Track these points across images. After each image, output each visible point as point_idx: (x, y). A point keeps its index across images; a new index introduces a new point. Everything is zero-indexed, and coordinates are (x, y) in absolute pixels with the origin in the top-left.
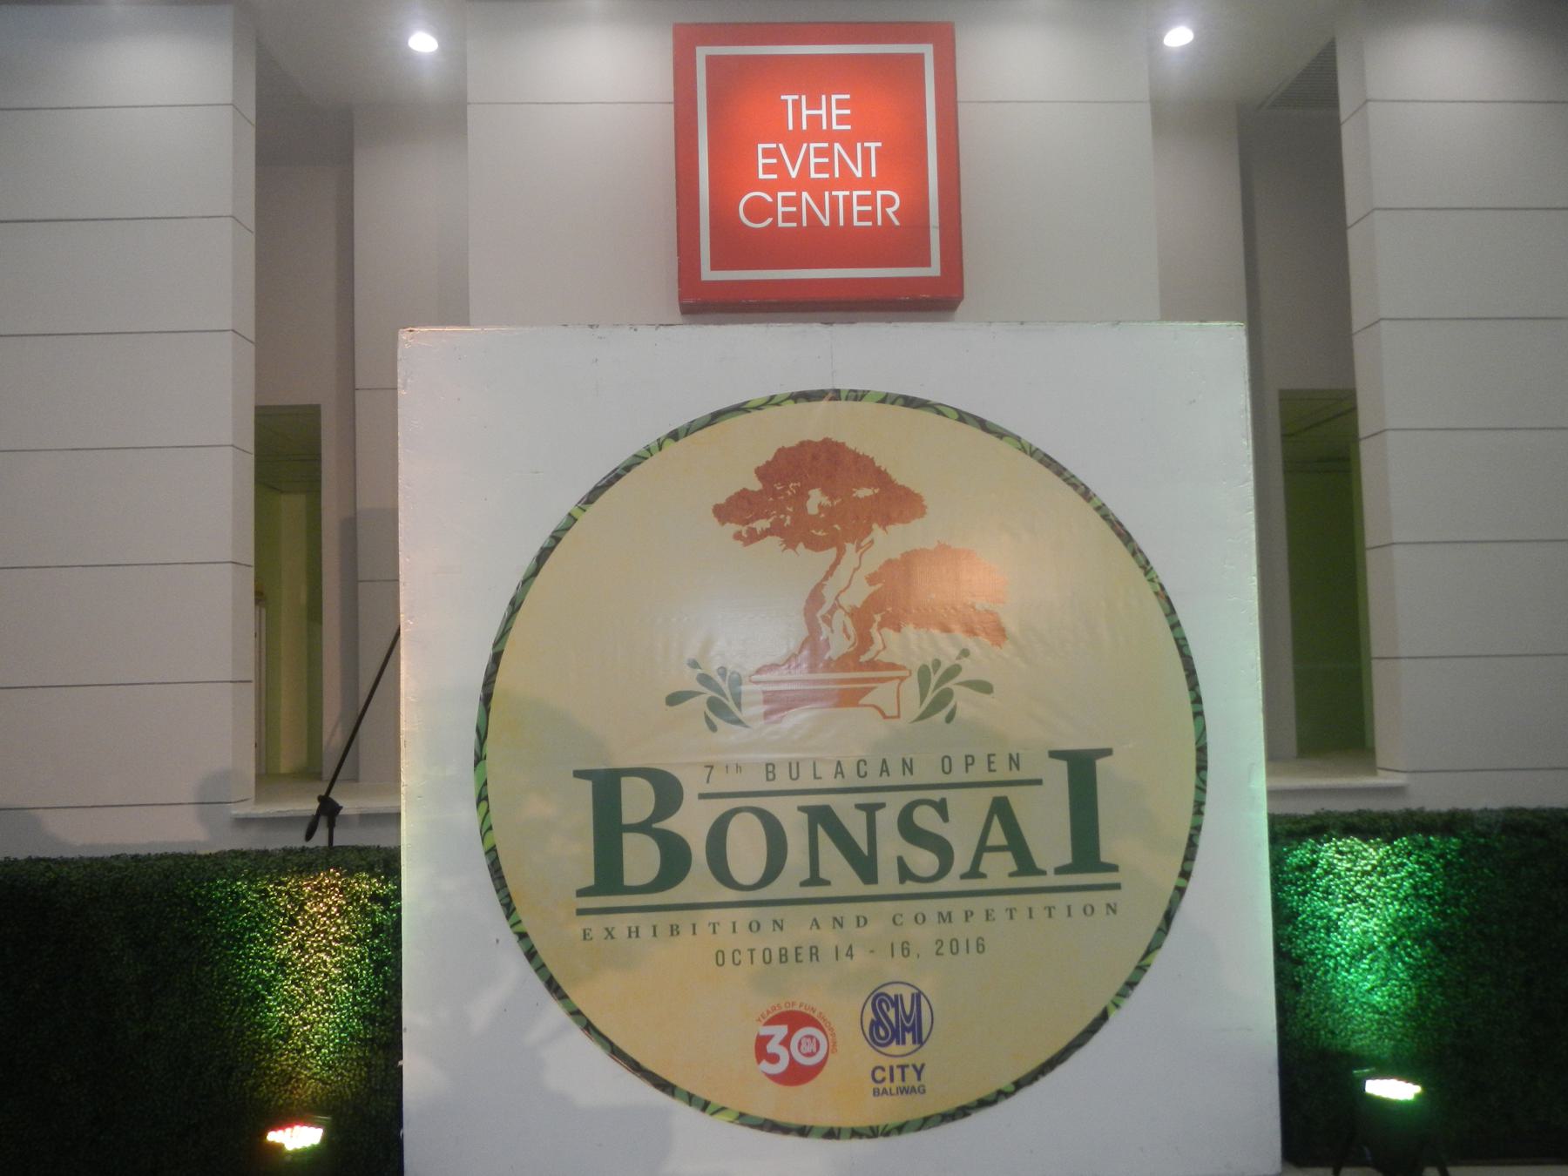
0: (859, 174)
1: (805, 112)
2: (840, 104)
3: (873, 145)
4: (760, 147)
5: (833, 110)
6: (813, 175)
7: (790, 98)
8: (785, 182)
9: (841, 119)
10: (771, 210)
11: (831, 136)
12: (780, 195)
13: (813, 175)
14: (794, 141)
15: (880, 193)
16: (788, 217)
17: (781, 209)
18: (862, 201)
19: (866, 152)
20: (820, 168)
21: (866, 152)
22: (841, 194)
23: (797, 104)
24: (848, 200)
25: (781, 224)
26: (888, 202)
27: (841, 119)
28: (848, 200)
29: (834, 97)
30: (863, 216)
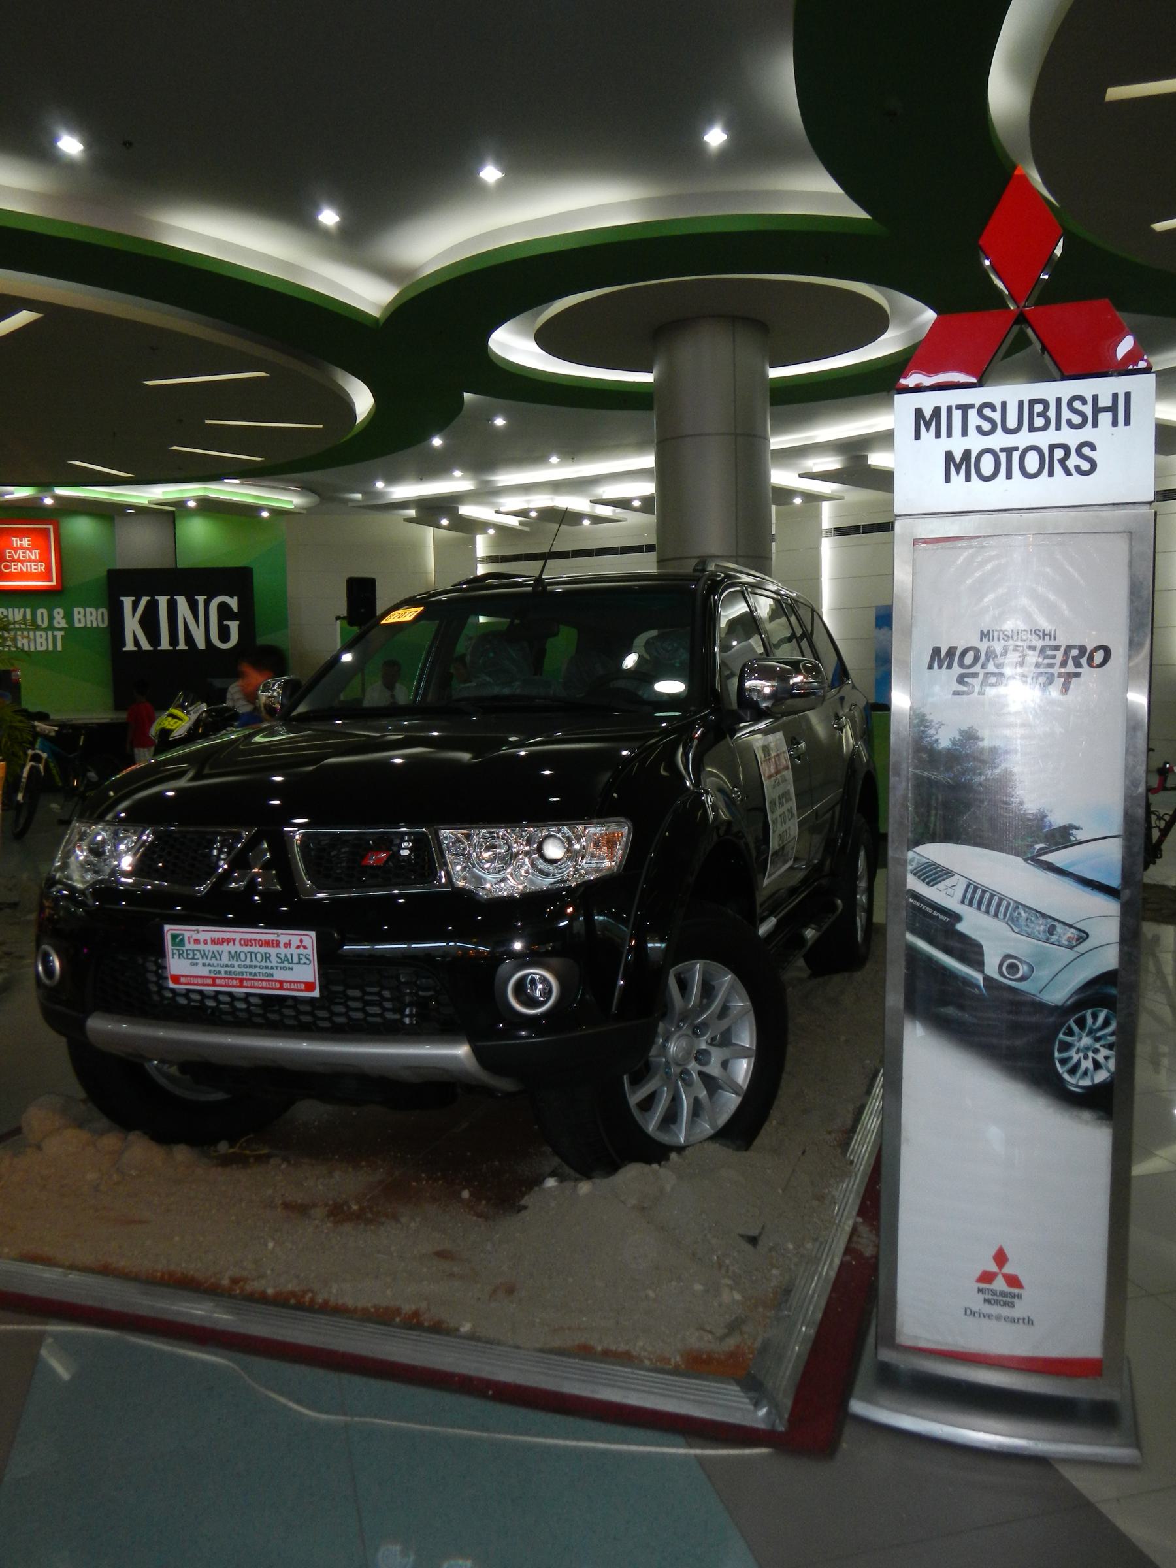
0: (33, 558)
1: (19, 542)
2: (28, 541)
3: (37, 551)
4: (7, 551)
5: (26, 542)
6: (21, 558)
7: (14, 539)
8: (14, 560)
9: (29, 544)
10: (10, 567)
11: (27, 549)
12: (13, 563)
13: (21, 558)
14: (16, 550)
15: (40, 563)
16: (15, 569)
17: (13, 567)
18: (35, 565)
19: (35, 553)
20: (23, 557)
21: (35, 553)
22: (29, 564)
23: (16, 541)
24: (31, 566)
25: (13, 571)
26: (41, 566)
27: (29, 544)
28: (31, 566)
29: (27, 539)
30: (35, 569)
